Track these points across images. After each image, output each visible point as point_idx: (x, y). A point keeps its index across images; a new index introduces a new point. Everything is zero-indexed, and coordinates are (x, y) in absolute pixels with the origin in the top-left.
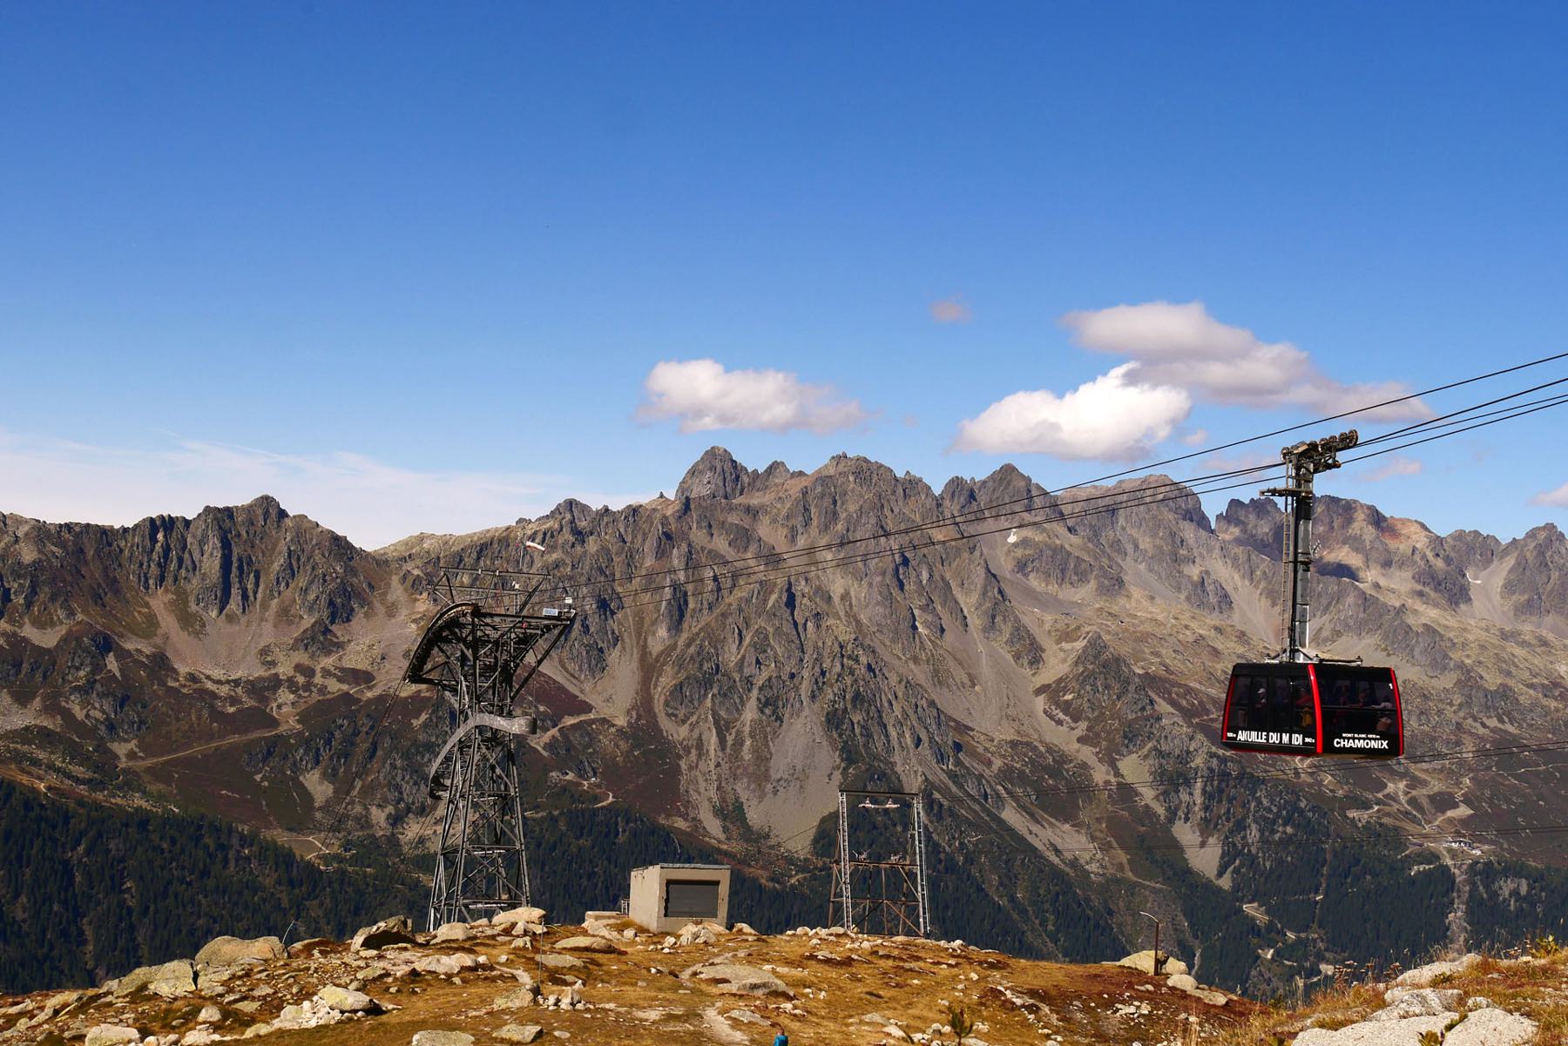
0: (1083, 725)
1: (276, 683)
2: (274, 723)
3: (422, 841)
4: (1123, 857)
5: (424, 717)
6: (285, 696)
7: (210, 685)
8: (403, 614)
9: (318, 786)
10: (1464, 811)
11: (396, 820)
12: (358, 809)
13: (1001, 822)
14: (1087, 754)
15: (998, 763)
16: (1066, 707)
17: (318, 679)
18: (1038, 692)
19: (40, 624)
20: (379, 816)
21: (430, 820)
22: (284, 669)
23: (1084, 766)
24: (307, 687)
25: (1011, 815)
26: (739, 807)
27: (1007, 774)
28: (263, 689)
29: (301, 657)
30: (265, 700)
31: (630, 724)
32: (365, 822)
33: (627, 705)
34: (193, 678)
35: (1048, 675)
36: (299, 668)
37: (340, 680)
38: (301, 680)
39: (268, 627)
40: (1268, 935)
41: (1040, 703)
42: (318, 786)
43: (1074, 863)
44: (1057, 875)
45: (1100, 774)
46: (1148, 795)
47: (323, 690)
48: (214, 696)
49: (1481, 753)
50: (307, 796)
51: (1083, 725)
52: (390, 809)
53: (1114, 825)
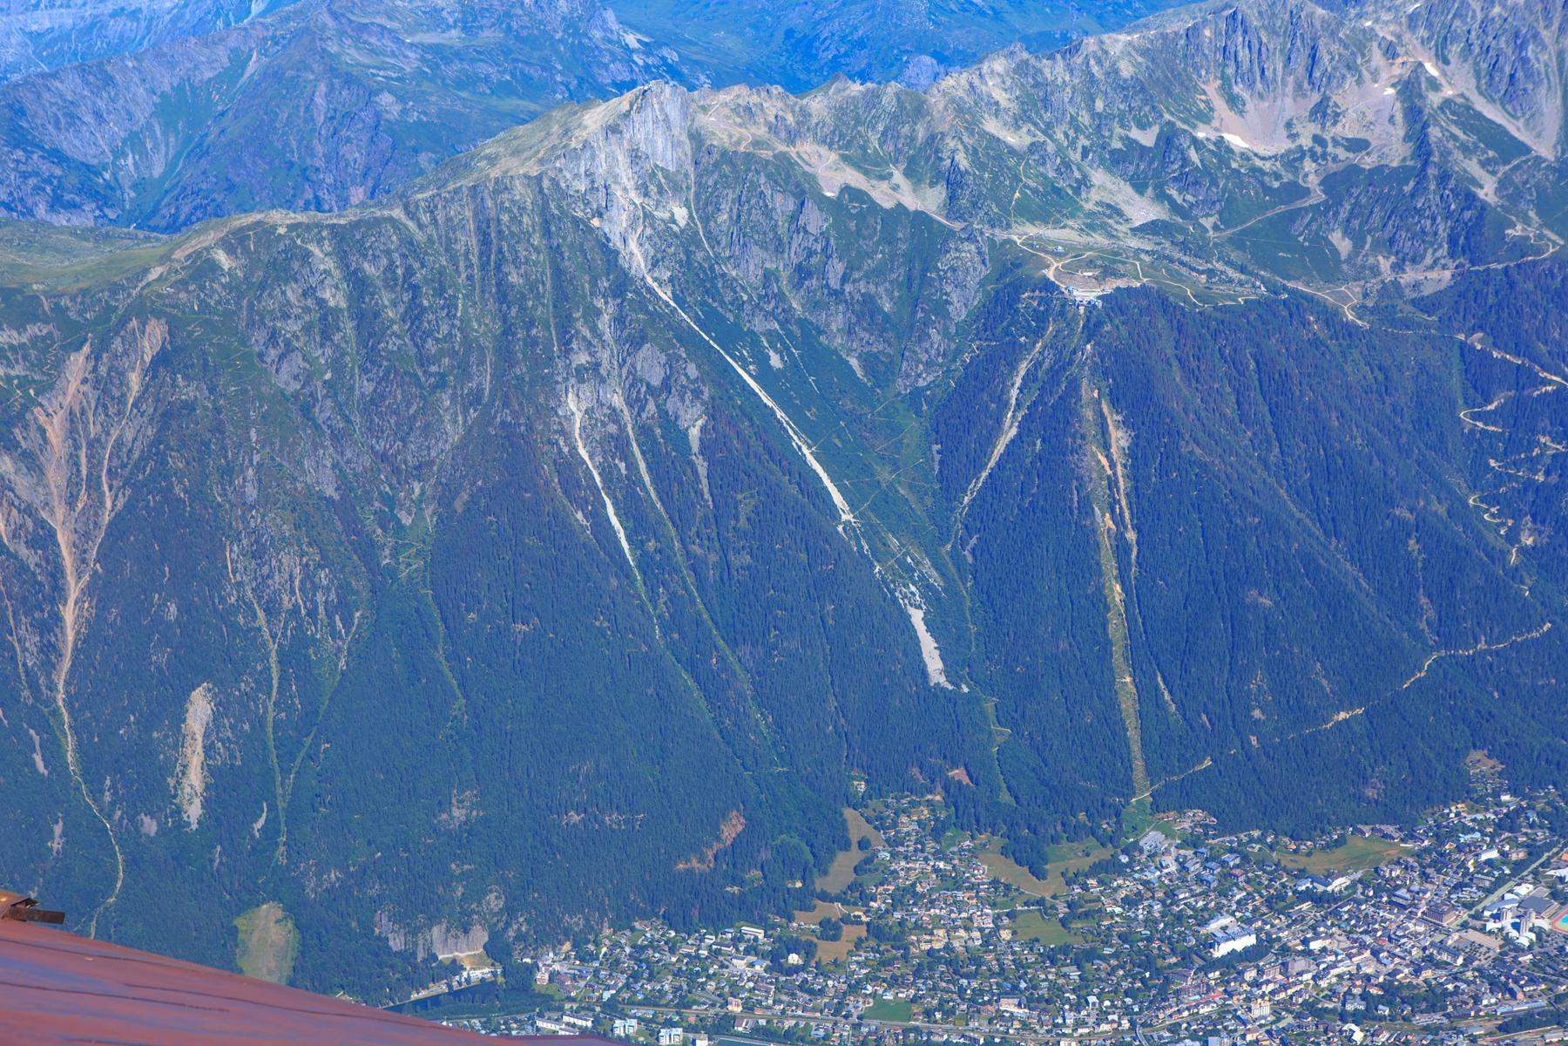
1: (1302, 154)
2: (1307, 192)
3: (1416, 286)
5: (1412, 184)
6: (1309, 165)
7: (1259, 163)
8: (1384, 75)
9: (1343, 245)
11: (1398, 267)
12: (1371, 260)
17: (1330, 149)
19: (1142, 126)
20: (1385, 264)
21: (1421, 267)
22: (1306, 142)
24: (1324, 156)
28: (1292, 160)
29: (1314, 128)
30: (1296, 171)
31: (1557, 160)
32: (1375, 271)
33: (1554, 139)
34: (1244, 156)
36: (1318, 139)
37: (1348, 149)
38: (1319, 150)
39: (1289, 101)
42: (1343, 245)
47: (1335, 159)
48: (1261, 171)
50: (1335, 252)
52: (1393, 259)
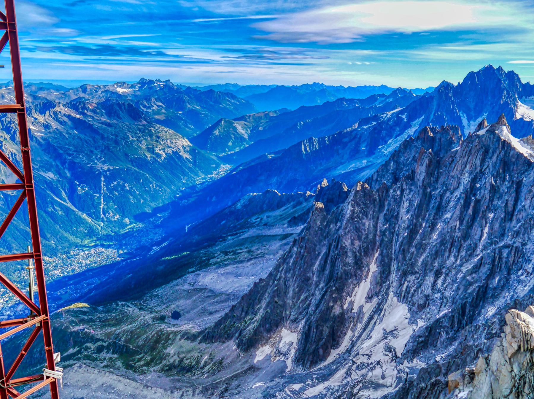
0: (50, 156)
4: (58, 176)
10: (103, 159)
13: (41, 175)
14: (51, 160)
15: (39, 165)
16: (47, 153)
18: (42, 150)
23: (51, 162)
25: (42, 174)
26: (3, 180)
27: (40, 166)
35: (43, 148)
40: (79, 185)
41: (43, 152)
43: (52, 179)
44: (51, 182)
45: (53, 163)
46: (60, 166)
49: (105, 148)
51: (50, 156)
53: (56, 171)
